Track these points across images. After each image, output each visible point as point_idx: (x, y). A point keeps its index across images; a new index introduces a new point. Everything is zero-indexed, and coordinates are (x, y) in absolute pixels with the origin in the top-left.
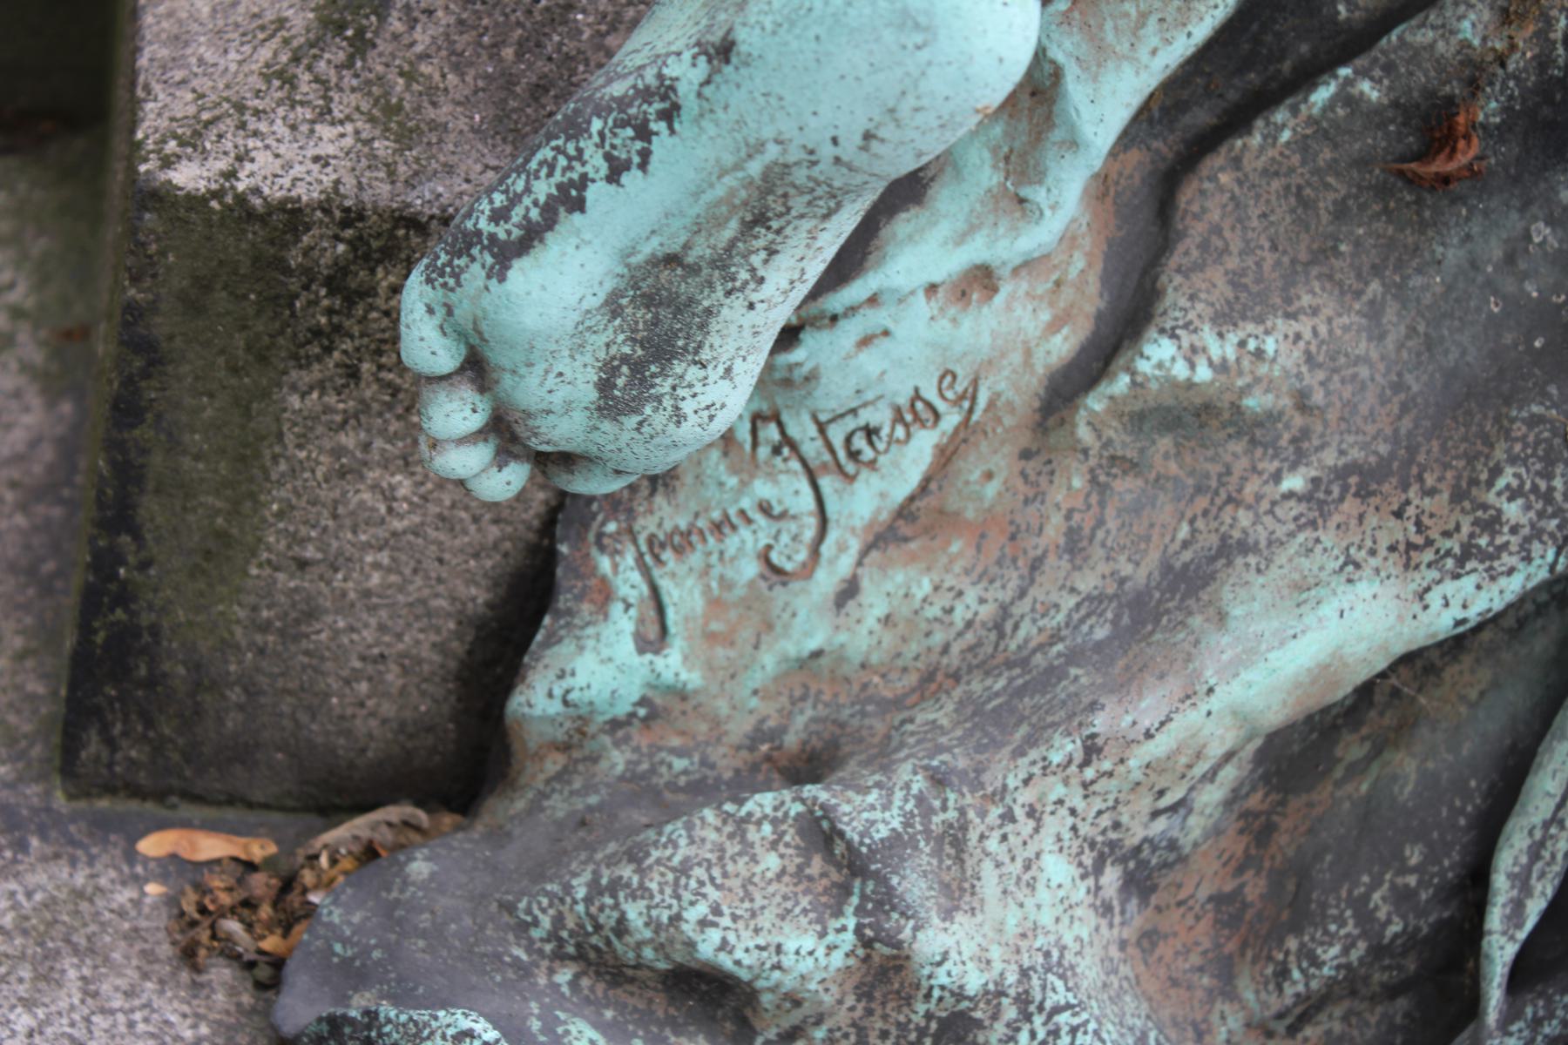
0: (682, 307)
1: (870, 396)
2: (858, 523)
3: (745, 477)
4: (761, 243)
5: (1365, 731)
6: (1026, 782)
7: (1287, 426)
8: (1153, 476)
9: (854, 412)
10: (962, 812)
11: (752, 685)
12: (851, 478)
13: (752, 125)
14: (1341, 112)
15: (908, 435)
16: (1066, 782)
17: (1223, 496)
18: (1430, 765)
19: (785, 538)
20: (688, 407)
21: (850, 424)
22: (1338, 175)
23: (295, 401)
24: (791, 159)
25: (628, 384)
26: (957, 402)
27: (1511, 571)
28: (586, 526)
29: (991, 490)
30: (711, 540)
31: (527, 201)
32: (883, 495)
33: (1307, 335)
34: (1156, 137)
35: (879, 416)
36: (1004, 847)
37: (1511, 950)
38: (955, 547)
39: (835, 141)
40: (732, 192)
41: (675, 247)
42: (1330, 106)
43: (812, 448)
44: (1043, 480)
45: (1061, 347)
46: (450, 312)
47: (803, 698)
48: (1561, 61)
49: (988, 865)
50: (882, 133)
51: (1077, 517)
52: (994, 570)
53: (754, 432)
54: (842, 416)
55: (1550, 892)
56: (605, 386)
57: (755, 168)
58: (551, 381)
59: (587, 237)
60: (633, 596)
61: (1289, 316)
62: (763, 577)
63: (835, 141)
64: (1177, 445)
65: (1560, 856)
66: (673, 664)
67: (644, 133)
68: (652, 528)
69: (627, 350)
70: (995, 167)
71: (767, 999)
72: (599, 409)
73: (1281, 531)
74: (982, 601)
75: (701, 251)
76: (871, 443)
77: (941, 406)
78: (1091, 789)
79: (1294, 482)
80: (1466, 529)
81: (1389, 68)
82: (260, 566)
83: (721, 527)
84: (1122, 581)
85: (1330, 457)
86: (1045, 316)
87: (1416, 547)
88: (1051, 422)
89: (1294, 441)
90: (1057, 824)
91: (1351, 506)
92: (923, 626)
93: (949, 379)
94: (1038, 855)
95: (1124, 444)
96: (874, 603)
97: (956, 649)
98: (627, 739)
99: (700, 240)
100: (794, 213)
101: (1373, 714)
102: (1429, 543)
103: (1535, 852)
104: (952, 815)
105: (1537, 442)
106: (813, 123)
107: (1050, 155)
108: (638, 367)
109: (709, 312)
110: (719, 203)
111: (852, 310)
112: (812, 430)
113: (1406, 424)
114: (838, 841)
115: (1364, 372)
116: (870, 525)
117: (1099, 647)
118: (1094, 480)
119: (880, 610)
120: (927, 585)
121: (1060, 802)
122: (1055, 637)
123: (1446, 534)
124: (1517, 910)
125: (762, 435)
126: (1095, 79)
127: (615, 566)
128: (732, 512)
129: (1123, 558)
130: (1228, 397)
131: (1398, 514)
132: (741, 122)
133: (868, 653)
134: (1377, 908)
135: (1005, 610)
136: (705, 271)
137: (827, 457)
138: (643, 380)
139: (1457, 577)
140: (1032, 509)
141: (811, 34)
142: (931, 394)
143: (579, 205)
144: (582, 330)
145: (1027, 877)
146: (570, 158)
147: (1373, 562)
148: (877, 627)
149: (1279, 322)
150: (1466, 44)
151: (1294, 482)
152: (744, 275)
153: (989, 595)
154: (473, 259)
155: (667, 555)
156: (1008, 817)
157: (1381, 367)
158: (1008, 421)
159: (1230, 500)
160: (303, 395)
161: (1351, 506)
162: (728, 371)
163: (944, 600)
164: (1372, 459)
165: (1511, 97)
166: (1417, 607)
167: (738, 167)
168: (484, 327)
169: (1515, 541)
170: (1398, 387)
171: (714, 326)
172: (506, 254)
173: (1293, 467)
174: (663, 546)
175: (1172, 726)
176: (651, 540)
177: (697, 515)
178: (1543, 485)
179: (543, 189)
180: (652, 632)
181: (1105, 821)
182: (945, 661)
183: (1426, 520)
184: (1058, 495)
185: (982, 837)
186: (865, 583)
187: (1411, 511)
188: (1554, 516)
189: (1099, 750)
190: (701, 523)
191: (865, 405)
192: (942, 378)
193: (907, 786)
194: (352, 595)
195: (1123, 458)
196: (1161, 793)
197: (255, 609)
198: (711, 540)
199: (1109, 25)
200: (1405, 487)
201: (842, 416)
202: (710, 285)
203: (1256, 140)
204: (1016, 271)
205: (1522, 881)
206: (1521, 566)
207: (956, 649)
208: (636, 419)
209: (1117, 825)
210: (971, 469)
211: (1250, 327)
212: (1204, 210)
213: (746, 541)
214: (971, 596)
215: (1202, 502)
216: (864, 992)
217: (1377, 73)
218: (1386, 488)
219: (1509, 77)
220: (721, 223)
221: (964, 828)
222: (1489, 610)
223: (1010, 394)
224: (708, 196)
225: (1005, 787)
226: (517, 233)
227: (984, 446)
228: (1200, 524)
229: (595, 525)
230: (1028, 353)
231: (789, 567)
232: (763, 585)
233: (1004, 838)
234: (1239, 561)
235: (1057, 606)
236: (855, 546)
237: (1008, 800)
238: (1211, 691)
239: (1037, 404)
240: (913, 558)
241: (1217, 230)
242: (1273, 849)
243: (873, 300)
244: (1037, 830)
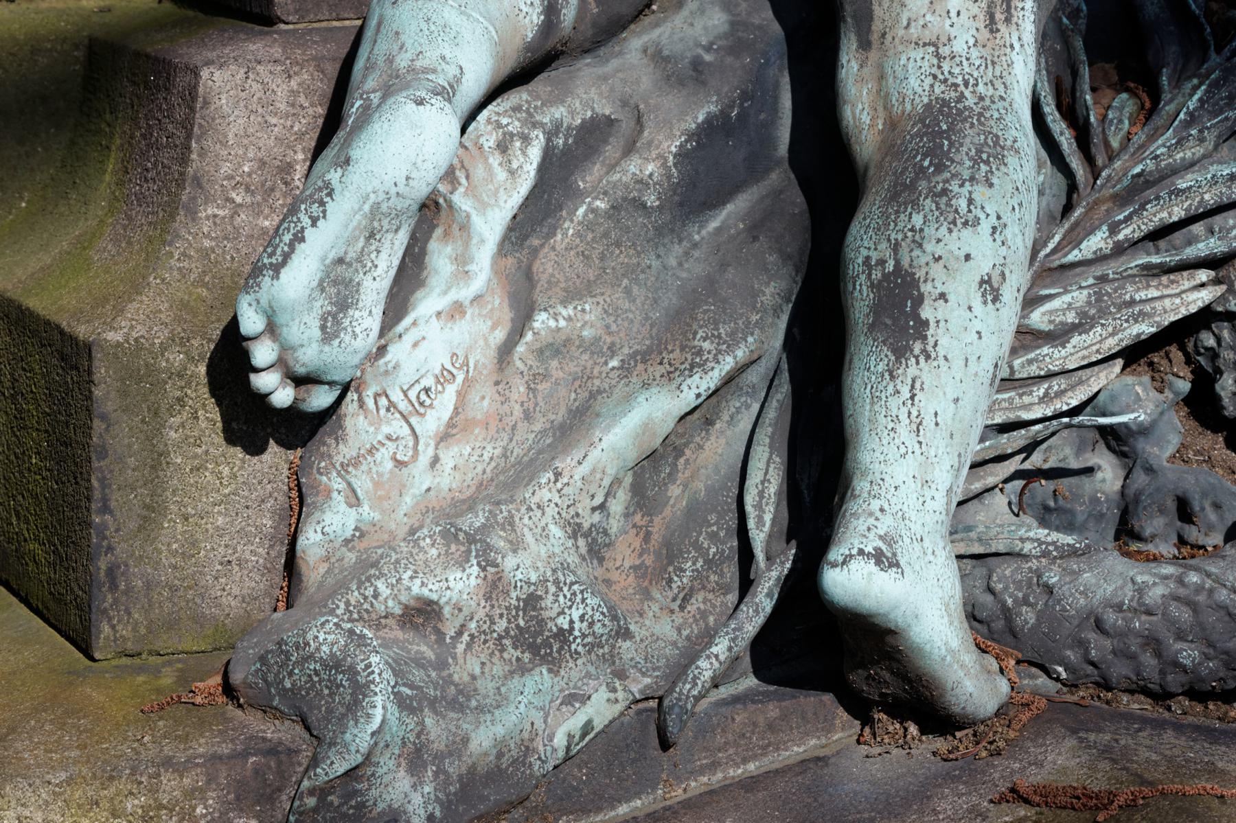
0: (348, 283)
1: (423, 371)
2: (432, 434)
3: (377, 426)
4: (373, 248)
5: (678, 482)
6: (533, 494)
7: (604, 343)
8: (553, 380)
9: (417, 381)
10: (509, 512)
11: (402, 513)
12: (422, 415)
13: (363, 188)
14: (591, 216)
15: (444, 389)
16: (550, 490)
17: (586, 378)
18: (709, 482)
19: (401, 448)
20: (358, 330)
21: (417, 388)
22: (597, 242)
23: (172, 434)
24: (380, 199)
25: (333, 325)
26: (460, 369)
27: (713, 369)
28: (312, 468)
29: (486, 403)
30: (369, 457)
31: (282, 245)
32: (439, 419)
33: (602, 302)
34: (517, 251)
35: (429, 382)
36: (531, 522)
37: (762, 536)
38: (476, 431)
39: (396, 185)
40: (360, 224)
41: (342, 254)
42: (586, 215)
43: (403, 405)
44: (507, 392)
45: (500, 335)
46: (258, 302)
47: (427, 512)
48: (676, 175)
49: (526, 530)
50: (412, 176)
51: (526, 404)
52: (496, 435)
53: (376, 403)
54: (413, 385)
55: (772, 510)
56: (323, 328)
57: (367, 208)
58: (302, 326)
59: (308, 253)
60: (340, 487)
61: (591, 297)
62: (396, 467)
63: (396, 185)
64: (560, 363)
65: (772, 495)
67: (322, 203)
68: (341, 459)
69: (329, 308)
70: (452, 263)
71: (447, 611)
72: (322, 340)
73: (614, 382)
74: (494, 448)
75: (352, 255)
76: (429, 396)
77: (454, 371)
78: (562, 492)
79: (614, 363)
80: (689, 358)
81: (605, 193)
82: (169, 522)
83: (372, 451)
84: (552, 422)
85: (626, 351)
86: (489, 323)
87: (671, 372)
88: (504, 365)
89: (609, 348)
90: (551, 511)
91: (640, 367)
92: (472, 466)
93: (455, 358)
94: (547, 525)
95: (538, 367)
97: (488, 470)
98: (354, 548)
99: (350, 249)
100: (384, 229)
101: (680, 474)
102: (676, 369)
103: (761, 494)
104: (505, 514)
105: (709, 319)
106: (386, 178)
107: (474, 249)
108: (334, 317)
109: (358, 284)
110: (355, 229)
111: (407, 330)
112: (401, 396)
113: (654, 331)
114: (460, 533)
115: (631, 316)
116: (436, 435)
117: (549, 445)
118: (529, 388)
119: (451, 464)
120: (469, 449)
121: (550, 501)
122: (529, 450)
123: (682, 363)
124: (760, 522)
125: (380, 404)
126: (484, 214)
127: (329, 479)
128: (375, 443)
129: (550, 414)
130: (576, 333)
131: (661, 363)
132: (359, 188)
133: (451, 483)
134: (702, 543)
135: (505, 449)
136: (354, 265)
137: (411, 408)
138: (338, 322)
139: (691, 376)
140: (505, 406)
141: (379, 142)
142: (449, 367)
143: (303, 240)
144: (311, 299)
145: (544, 534)
146: (295, 223)
147: (655, 383)
148: (451, 472)
149: (589, 299)
150: (634, 174)
151: (614, 363)
152: (369, 264)
153: (497, 445)
154: (264, 276)
155: (350, 469)
156: (530, 509)
157: (638, 312)
158: (485, 372)
159: (589, 378)
160: (176, 431)
161: (640, 367)
162: (370, 312)
163: (479, 452)
164: (644, 347)
165: (659, 193)
166: (678, 392)
167: (360, 209)
168: (273, 304)
169: (711, 357)
170: (647, 318)
171: (362, 291)
172: (277, 269)
173: (612, 358)
174: (348, 465)
175: (588, 458)
176: (342, 465)
177: (359, 449)
178: (716, 333)
179: (287, 238)
180: (353, 500)
181: (572, 511)
182: (485, 476)
183: (673, 362)
184: (515, 396)
185: (521, 519)
186: (441, 456)
187: (666, 361)
188: (724, 344)
189: (560, 474)
190: (362, 452)
191: (422, 377)
192: (452, 357)
193: (484, 509)
194: (211, 531)
195: (538, 374)
196: (593, 496)
197: (169, 545)
198: (369, 457)
199: (484, 195)
200: (661, 353)
201: (413, 385)
202: (357, 270)
203: (559, 237)
204: (472, 302)
205: (759, 507)
206: (716, 366)
207: (488, 470)
208: (338, 341)
209: (577, 515)
210: (474, 397)
211: (577, 302)
212: (545, 270)
213: (384, 455)
214: (489, 448)
215: (577, 383)
216: (488, 598)
217: (601, 196)
218: (653, 356)
219: (655, 184)
220: (357, 239)
221: (512, 517)
222: (709, 388)
223: (483, 360)
224: (350, 228)
225: (525, 498)
226: (280, 259)
227: (478, 386)
228: (579, 391)
229: (315, 466)
230: (486, 340)
231: (406, 459)
232: (397, 470)
233: (530, 518)
234: (599, 397)
235: (527, 439)
236: (432, 443)
237: (528, 503)
238: (600, 440)
239: (496, 361)
240: (459, 441)
241: (552, 275)
242: (653, 542)
243: (414, 323)
244: (543, 514)
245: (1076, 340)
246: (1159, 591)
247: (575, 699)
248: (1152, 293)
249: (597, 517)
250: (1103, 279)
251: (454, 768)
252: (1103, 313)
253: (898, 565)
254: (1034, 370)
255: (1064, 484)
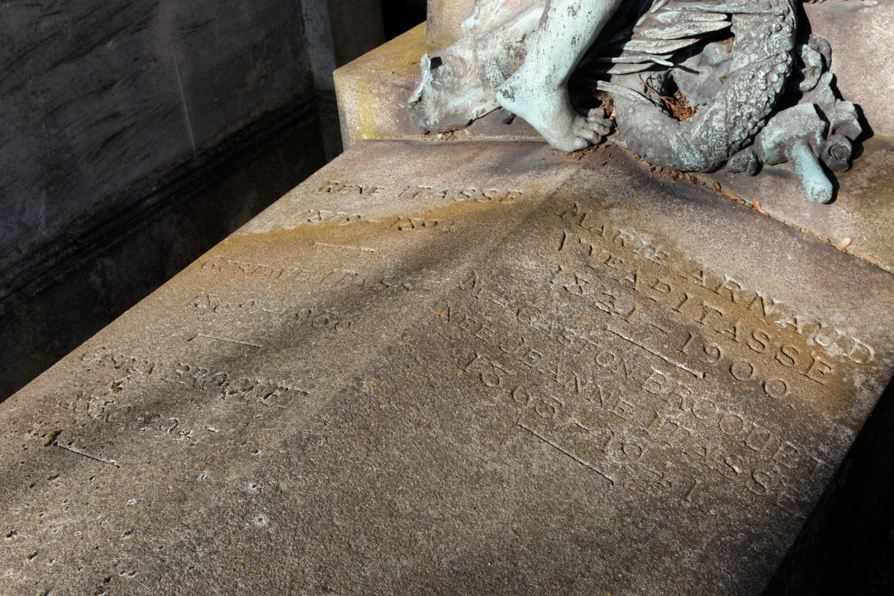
66: (478, 22)
90: (500, 40)
96: (499, 13)
245: (667, 29)
246: (649, 128)
247: (484, 100)
248: (703, 19)
249: (519, 45)
250: (684, 9)
251: (444, 111)
252: (679, 22)
253: (513, 97)
254: (651, 36)
255: (692, 74)
